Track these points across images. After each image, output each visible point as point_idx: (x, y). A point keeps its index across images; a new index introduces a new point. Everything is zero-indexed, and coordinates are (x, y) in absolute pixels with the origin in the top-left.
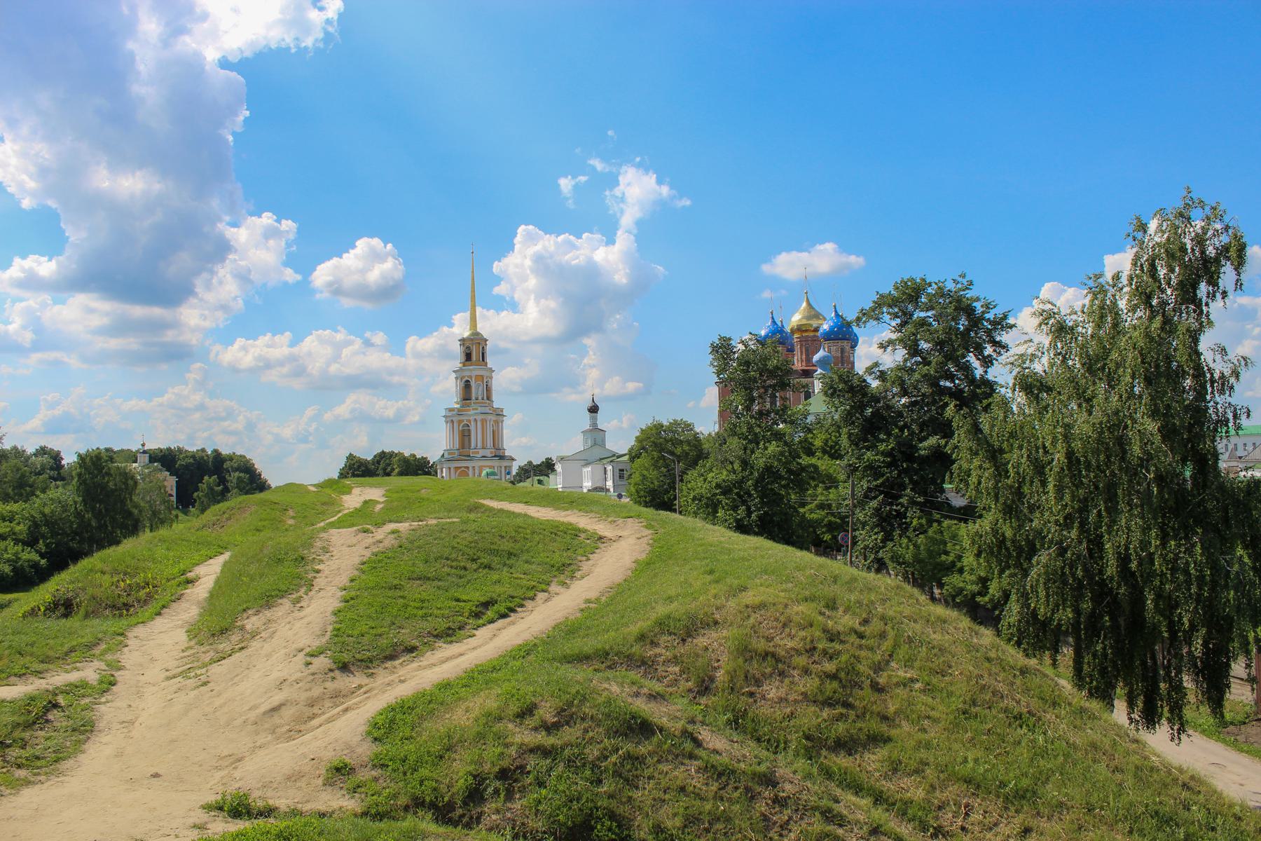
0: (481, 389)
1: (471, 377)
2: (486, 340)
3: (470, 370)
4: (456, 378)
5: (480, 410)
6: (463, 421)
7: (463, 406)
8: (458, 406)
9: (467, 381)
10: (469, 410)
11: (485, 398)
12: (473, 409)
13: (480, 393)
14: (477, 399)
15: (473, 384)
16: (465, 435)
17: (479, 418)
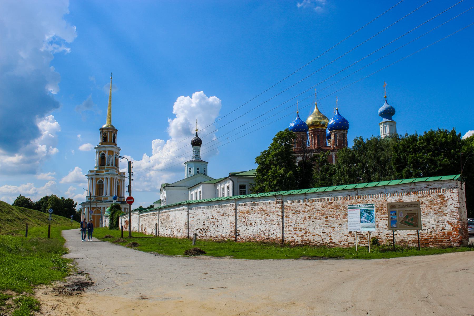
0: (111, 159)
1: (105, 152)
2: (117, 131)
3: (106, 147)
4: (97, 152)
5: (110, 172)
6: (99, 178)
7: (99, 169)
8: (96, 169)
9: (103, 154)
10: (103, 172)
11: (114, 165)
12: (106, 171)
13: (111, 161)
14: (108, 165)
15: (106, 156)
16: (100, 188)
17: (109, 177)
